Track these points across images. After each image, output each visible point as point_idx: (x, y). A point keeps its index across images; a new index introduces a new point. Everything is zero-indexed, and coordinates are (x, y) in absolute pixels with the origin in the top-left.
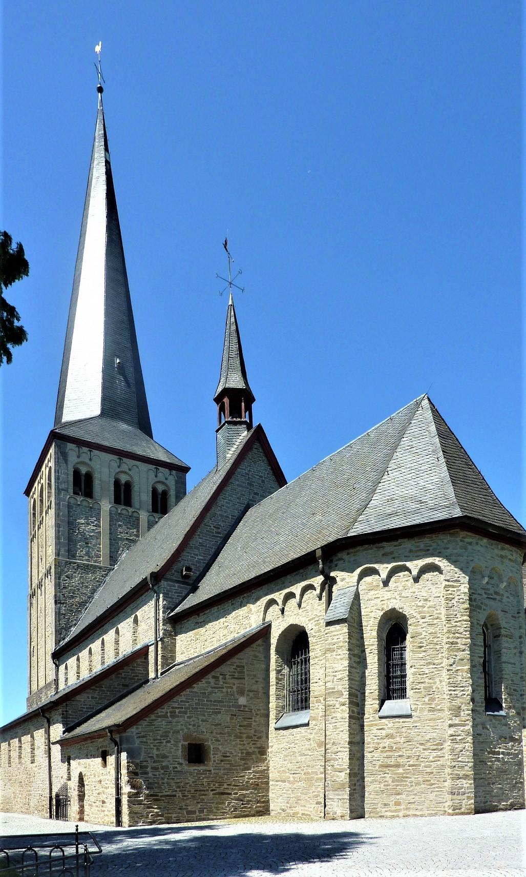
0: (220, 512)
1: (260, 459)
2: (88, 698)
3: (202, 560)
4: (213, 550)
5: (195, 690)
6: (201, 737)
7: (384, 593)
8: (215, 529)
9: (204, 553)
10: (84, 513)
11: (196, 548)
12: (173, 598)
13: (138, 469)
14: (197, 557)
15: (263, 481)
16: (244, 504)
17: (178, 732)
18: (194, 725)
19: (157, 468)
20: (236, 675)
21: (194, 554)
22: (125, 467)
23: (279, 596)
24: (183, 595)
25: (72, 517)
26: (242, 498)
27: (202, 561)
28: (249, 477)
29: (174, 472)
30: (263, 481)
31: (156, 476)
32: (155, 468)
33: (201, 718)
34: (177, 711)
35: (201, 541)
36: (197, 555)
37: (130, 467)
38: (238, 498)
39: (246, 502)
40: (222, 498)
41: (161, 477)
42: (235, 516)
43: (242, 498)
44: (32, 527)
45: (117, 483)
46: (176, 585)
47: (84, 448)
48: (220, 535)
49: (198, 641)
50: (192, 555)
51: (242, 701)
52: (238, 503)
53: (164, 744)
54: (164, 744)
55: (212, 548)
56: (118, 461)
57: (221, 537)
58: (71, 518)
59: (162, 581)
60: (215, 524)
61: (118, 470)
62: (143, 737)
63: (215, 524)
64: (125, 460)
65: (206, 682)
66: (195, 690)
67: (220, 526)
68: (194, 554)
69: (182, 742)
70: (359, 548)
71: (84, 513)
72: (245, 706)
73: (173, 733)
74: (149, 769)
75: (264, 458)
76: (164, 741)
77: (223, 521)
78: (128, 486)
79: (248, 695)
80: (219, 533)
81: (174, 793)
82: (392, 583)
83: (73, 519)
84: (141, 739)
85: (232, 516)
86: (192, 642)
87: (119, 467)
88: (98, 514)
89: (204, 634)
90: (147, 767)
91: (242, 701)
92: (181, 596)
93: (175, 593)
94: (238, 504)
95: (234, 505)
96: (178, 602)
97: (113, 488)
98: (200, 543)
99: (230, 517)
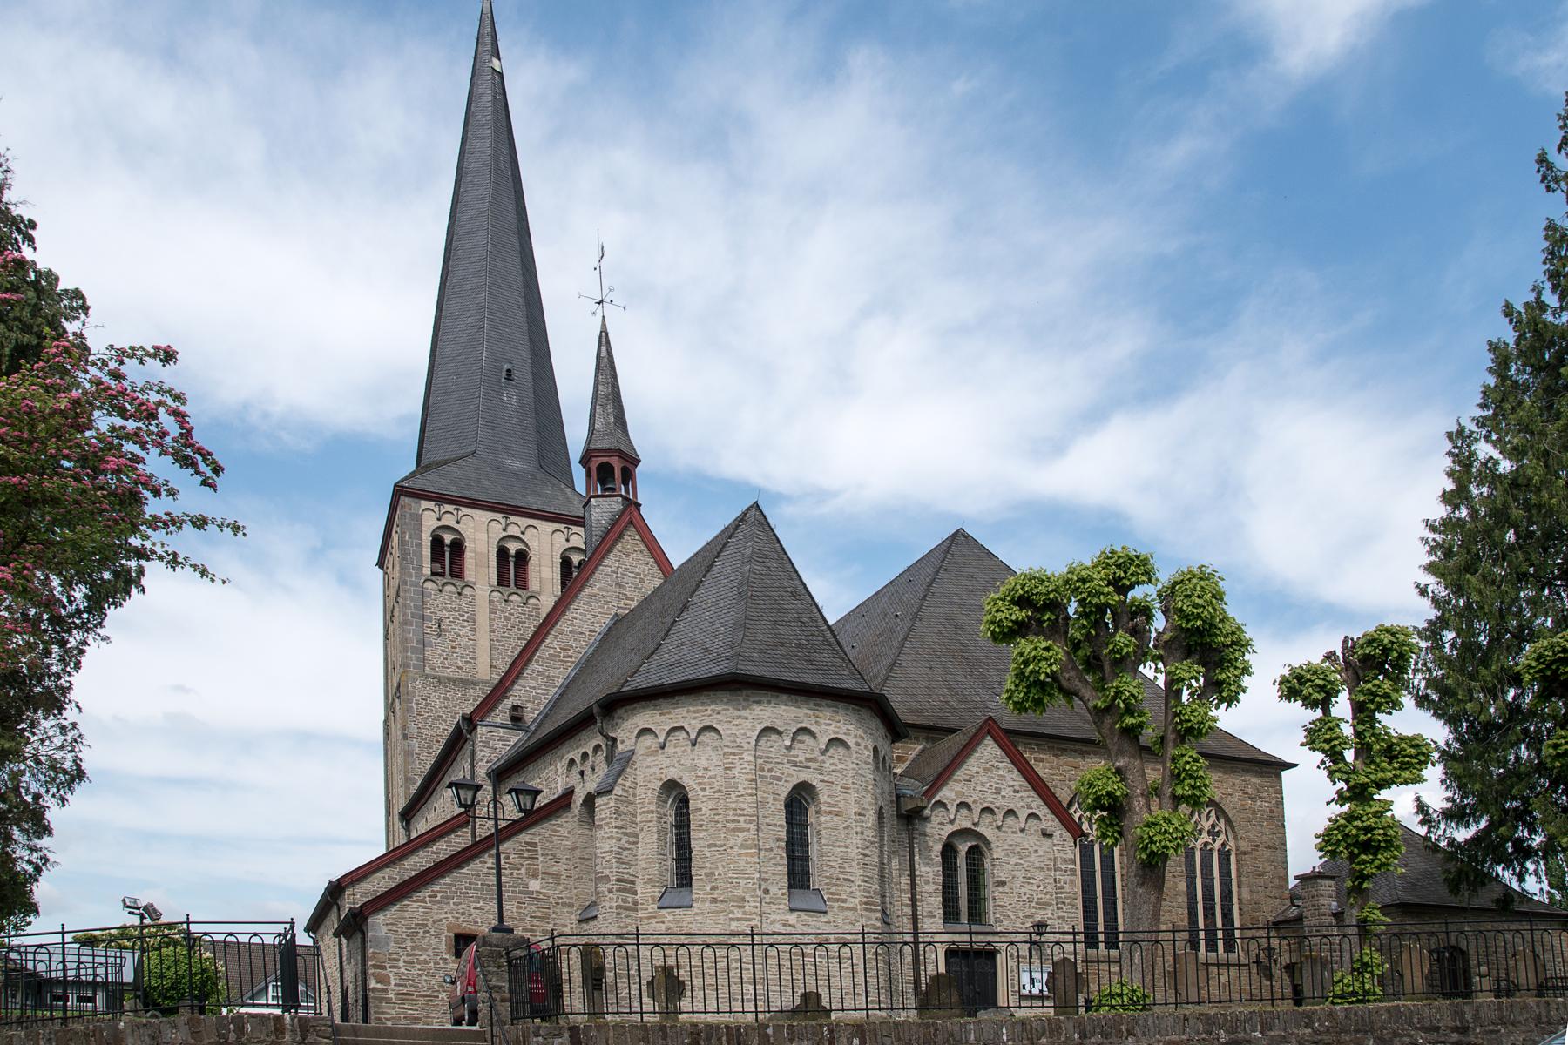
2: (384, 878)
4: (561, 681)
6: (473, 927)
7: (661, 759)
11: (533, 679)
15: (642, 581)
17: (441, 920)
18: (463, 914)
20: (526, 854)
21: (530, 688)
23: (576, 754)
24: (512, 743)
33: (473, 905)
34: (439, 895)
36: (534, 688)
37: (523, 530)
38: (599, 607)
39: (613, 612)
45: (502, 553)
46: (501, 730)
47: (446, 506)
51: (534, 885)
53: (421, 934)
54: (421, 934)
55: (558, 677)
57: (572, 662)
61: (504, 534)
62: (392, 924)
64: (513, 519)
65: (481, 862)
67: (572, 646)
69: (446, 934)
70: (635, 705)
72: (537, 892)
73: (434, 922)
74: (401, 964)
75: (643, 548)
76: (421, 931)
77: (575, 640)
78: (522, 558)
79: (542, 879)
81: (436, 994)
82: (669, 749)
84: (390, 927)
87: (504, 530)
90: (398, 960)
91: (534, 885)
95: (594, 616)
97: (493, 563)
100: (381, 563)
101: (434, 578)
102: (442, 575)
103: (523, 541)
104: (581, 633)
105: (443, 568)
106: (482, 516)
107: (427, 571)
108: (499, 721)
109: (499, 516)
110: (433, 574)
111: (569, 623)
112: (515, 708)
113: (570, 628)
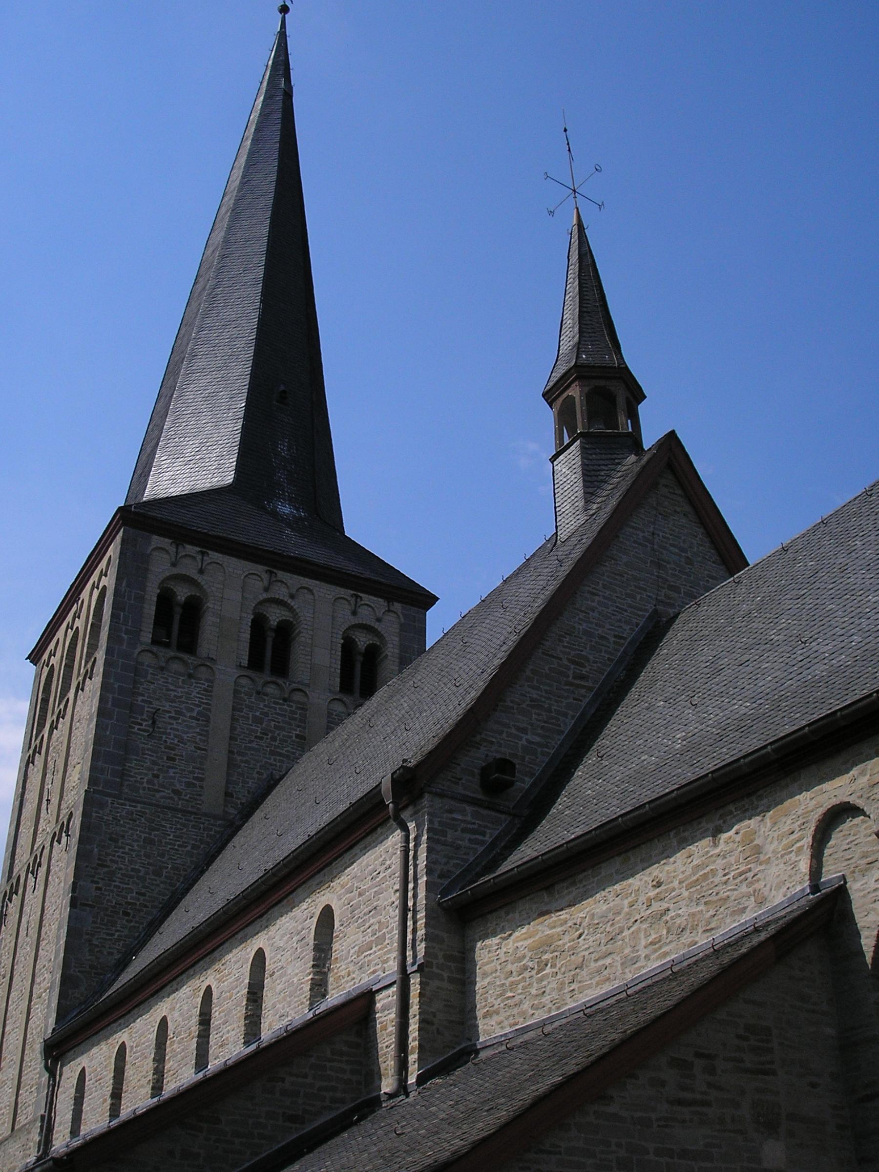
0: (584, 626)
1: (678, 509)
3: (539, 744)
5: (613, 1109)
8: (572, 666)
9: (543, 727)
10: (172, 687)
12: (458, 848)
13: (311, 597)
14: (525, 737)
16: (646, 610)
19: (357, 596)
21: (519, 729)
22: (280, 592)
24: (488, 839)
25: (143, 695)
26: (638, 597)
27: (539, 750)
28: (653, 550)
29: (397, 606)
30: (689, 561)
31: (354, 613)
32: (352, 595)
35: (534, 694)
36: (524, 731)
37: (294, 591)
38: (628, 595)
39: (650, 608)
40: (589, 592)
41: (365, 616)
42: (625, 639)
43: (638, 597)
44: (34, 733)
45: (258, 624)
46: (469, 809)
48: (586, 684)
49: (548, 970)
50: (513, 731)
52: (630, 606)
55: (565, 715)
56: (265, 576)
57: (590, 689)
58: (140, 698)
59: (427, 796)
60: (573, 653)
61: (265, 596)
63: (573, 653)
64: (281, 574)
66: (613, 1109)
67: (588, 660)
68: (519, 729)
71: (172, 687)
80: (583, 677)
83: (143, 701)
85: (615, 636)
86: (527, 974)
87: (266, 590)
88: (205, 690)
89: (573, 948)
92: (477, 842)
93: (464, 831)
94: (629, 610)
96: (472, 859)
97: (246, 636)
98: (532, 700)
99: (612, 639)
100: (35, 657)
101: (155, 649)
102: (167, 645)
103: (290, 608)
104: (602, 637)
105: (169, 636)
106: (236, 567)
107: (147, 637)
108: (460, 790)
109: (260, 569)
110: (155, 642)
111: (582, 615)
112: (505, 765)
113: (584, 626)
